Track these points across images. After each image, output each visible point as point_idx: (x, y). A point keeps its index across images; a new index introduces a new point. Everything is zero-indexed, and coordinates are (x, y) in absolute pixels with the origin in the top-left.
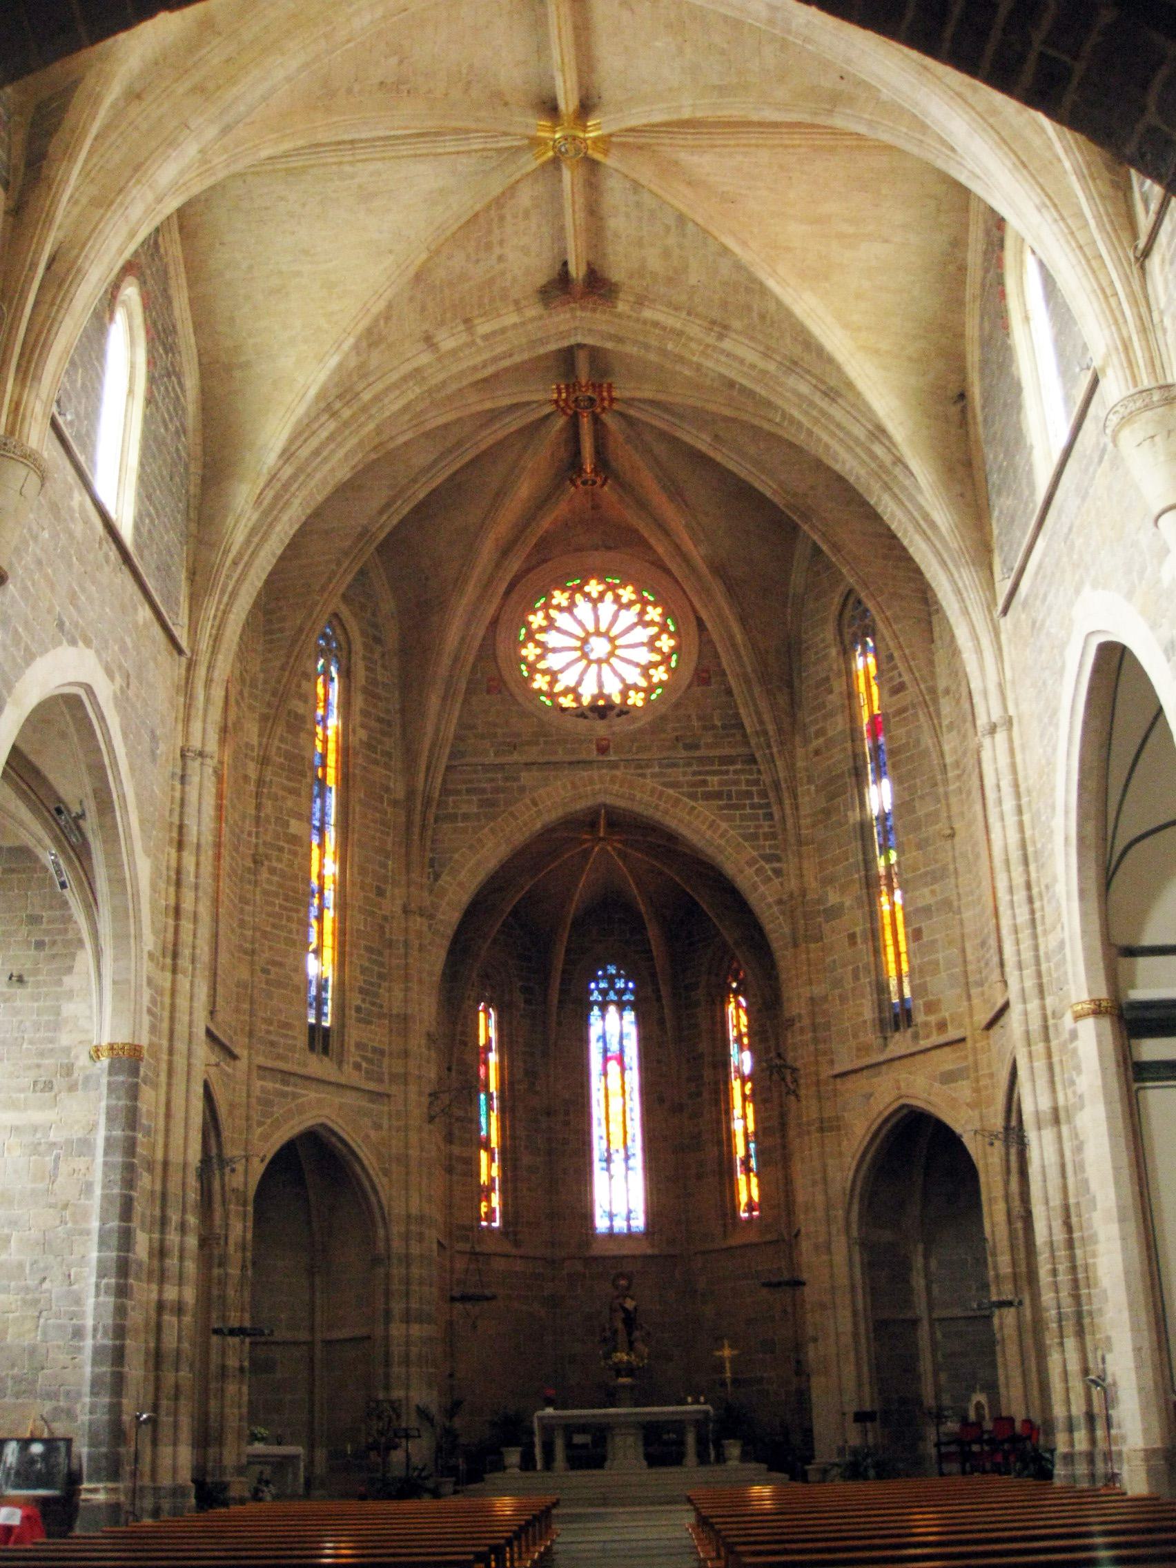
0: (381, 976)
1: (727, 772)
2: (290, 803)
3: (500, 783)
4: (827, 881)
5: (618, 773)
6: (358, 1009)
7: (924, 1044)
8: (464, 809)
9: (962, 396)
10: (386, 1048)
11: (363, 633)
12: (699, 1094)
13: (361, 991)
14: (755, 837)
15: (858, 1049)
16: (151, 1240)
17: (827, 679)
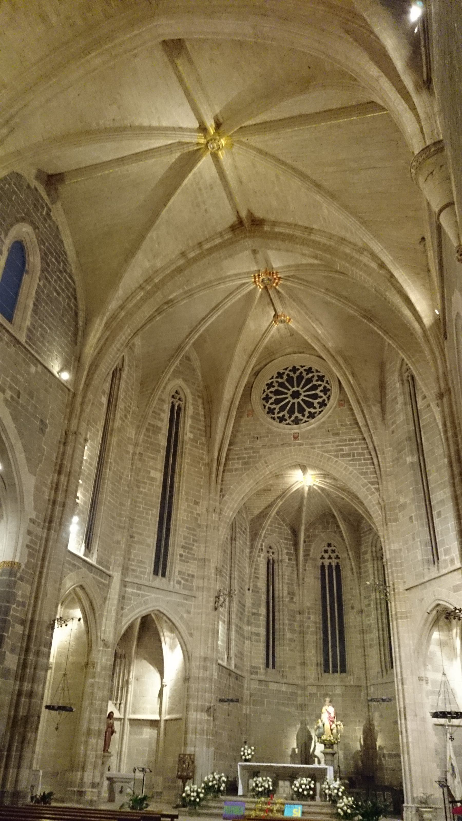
0: (194, 540)
1: (352, 445)
2: (151, 464)
3: (252, 455)
4: (399, 492)
5: (301, 447)
6: (181, 556)
7: (444, 571)
8: (236, 466)
9: (423, 239)
10: (196, 574)
11: (193, 394)
12: (369, 605)
13: (183, 547)
14: (366, 473)
15: (417, 576)
16: (19, 659)
17: (396, 398)
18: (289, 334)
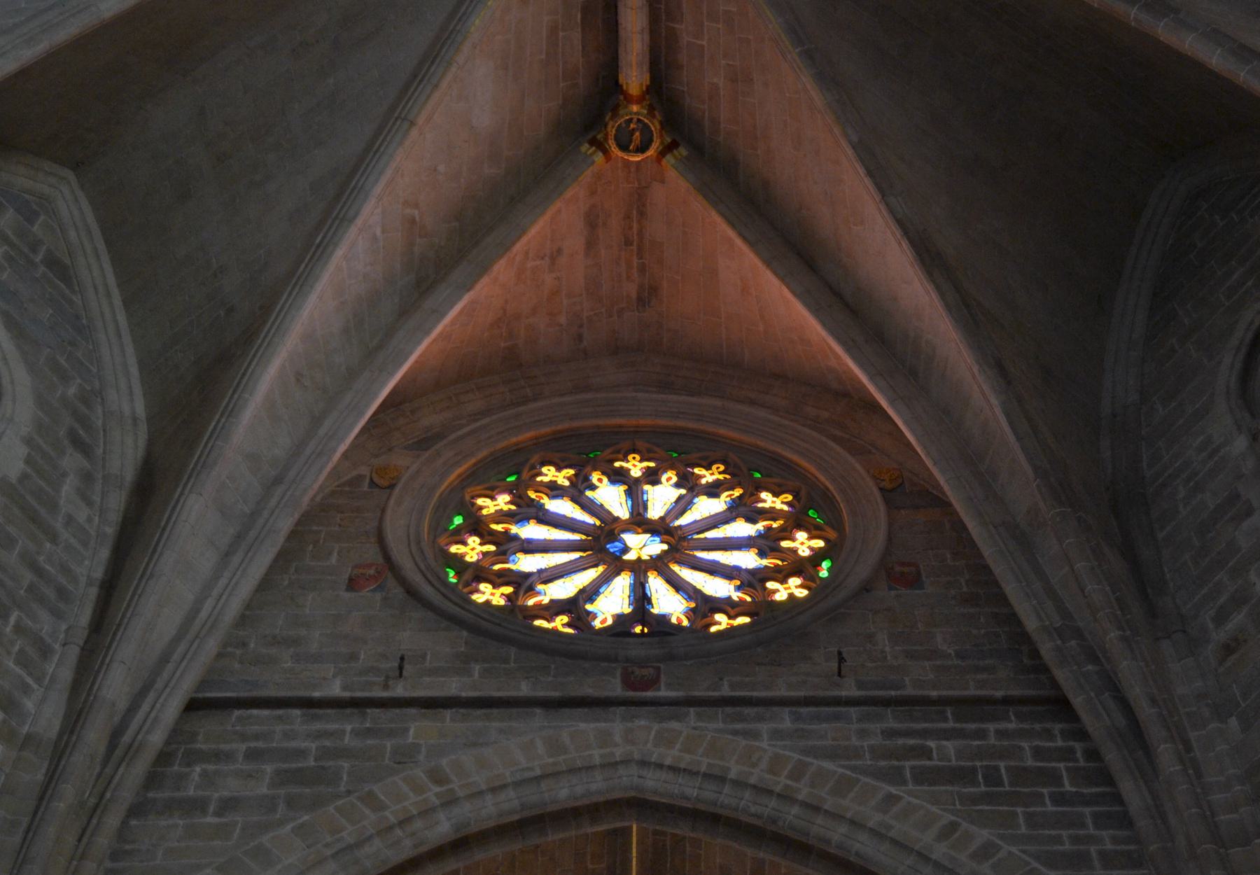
1: (981, 735)
8: (231, 787)
18: (631, 289)
